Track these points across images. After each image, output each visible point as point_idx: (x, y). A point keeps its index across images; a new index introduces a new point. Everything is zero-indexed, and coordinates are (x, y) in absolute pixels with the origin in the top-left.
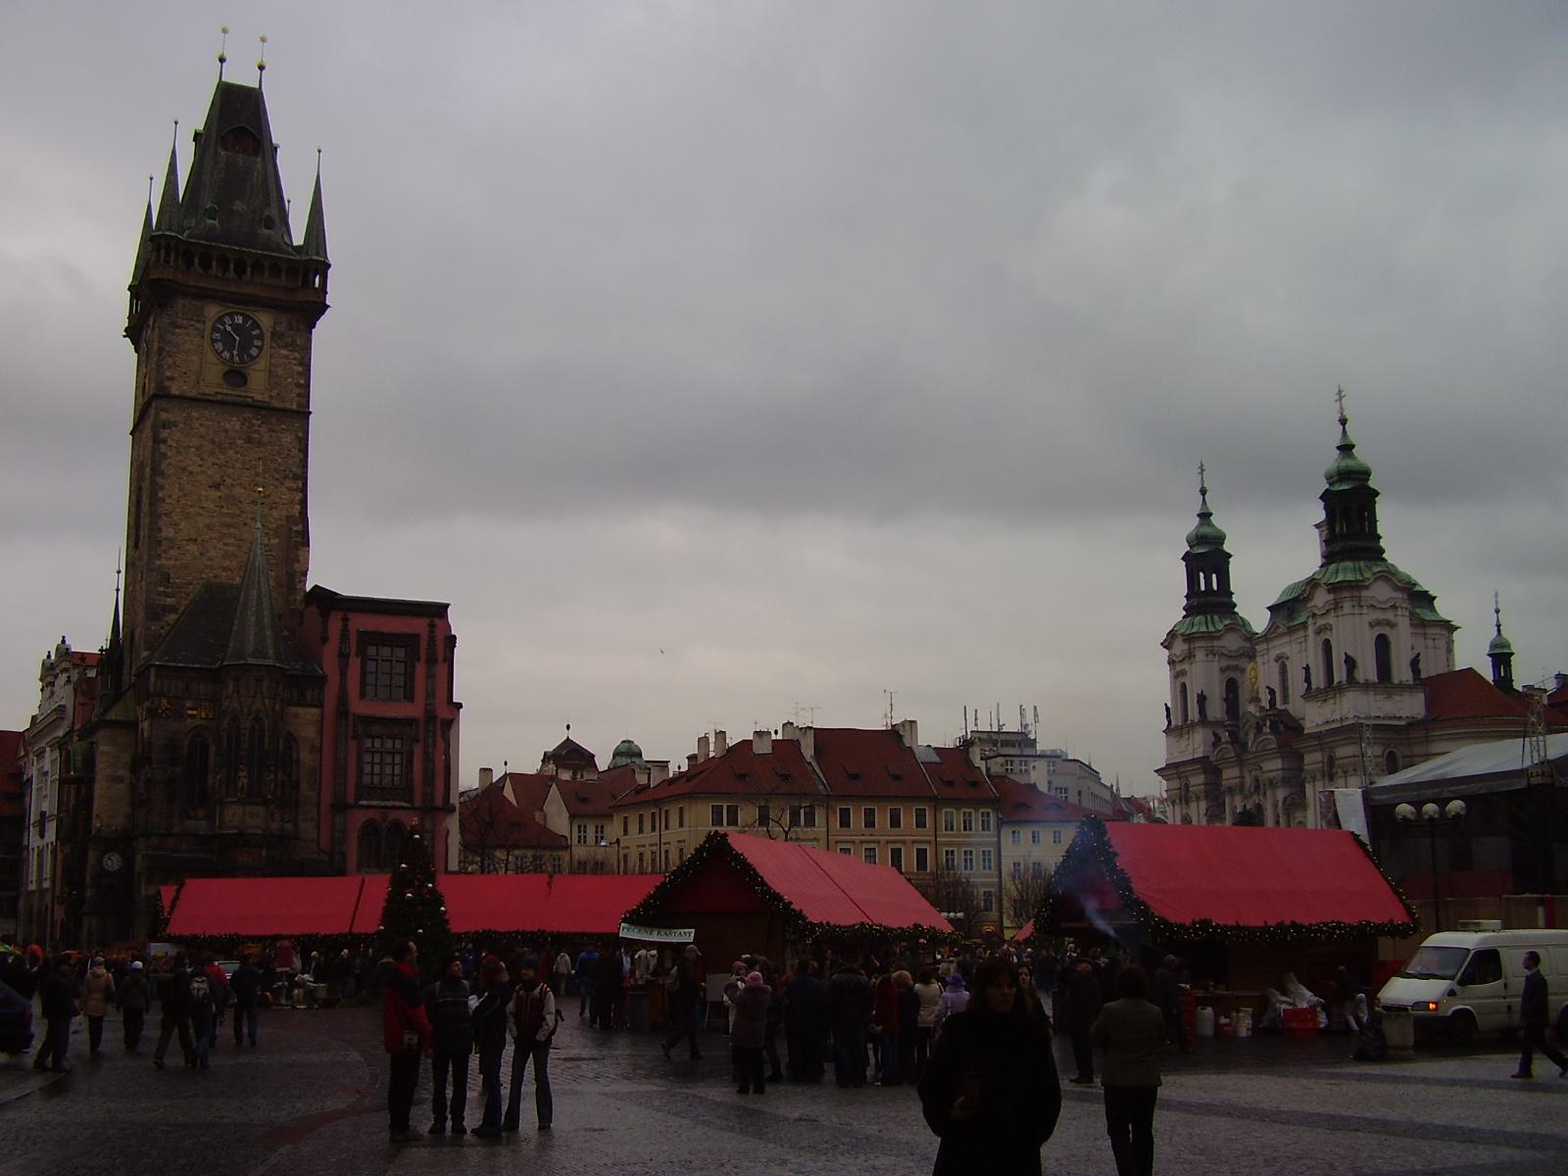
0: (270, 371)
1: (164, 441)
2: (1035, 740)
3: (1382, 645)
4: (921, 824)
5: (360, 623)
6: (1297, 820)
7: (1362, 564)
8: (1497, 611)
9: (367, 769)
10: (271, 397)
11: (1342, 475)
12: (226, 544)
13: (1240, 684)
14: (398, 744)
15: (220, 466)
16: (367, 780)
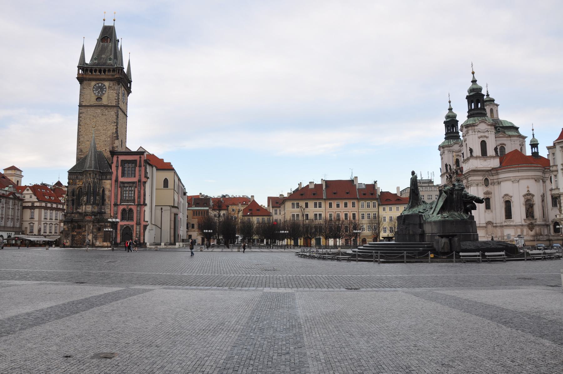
1: (81, 117)
2: (433, 182)
3: (483, 145)
7: (476, 118)
8: (533, 130)
11: (471, 90)
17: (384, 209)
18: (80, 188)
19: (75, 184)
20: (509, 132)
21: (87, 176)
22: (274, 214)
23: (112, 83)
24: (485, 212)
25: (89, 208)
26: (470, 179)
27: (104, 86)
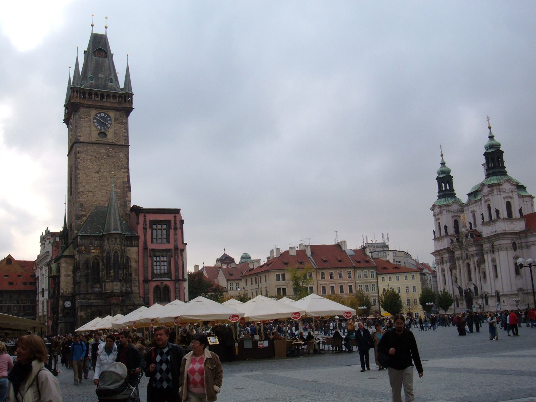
0: (114, 132)
1: (79, 158)
2: (388, 245)
3: (509, 205)
4: (350, 277)
5: (150, 217)
6: (482, 268)
7: (499, 177)
9: (155, 267)
10: (115, 141)
11: (491, 146)
12: (102, 192)
13: (459, 221)
14: (165, 258)
15: (99, 166)
16: (155, 271)
17: (383, 279)
18: (96, 258)
19: (89, 252)
20: (520, 192)
21: (112, 241)
22: (229, 288)
23: (118, 113)
24: (516, 278)
25: (117, 285)
26: (496, 243)
27: (107, 117)
